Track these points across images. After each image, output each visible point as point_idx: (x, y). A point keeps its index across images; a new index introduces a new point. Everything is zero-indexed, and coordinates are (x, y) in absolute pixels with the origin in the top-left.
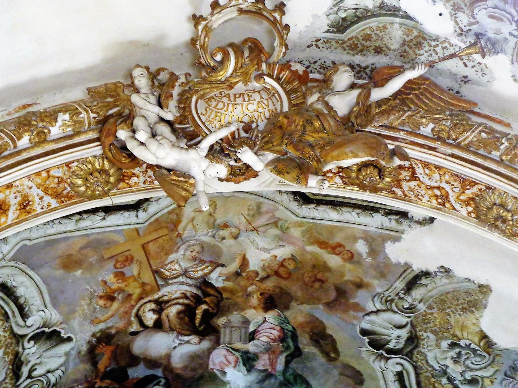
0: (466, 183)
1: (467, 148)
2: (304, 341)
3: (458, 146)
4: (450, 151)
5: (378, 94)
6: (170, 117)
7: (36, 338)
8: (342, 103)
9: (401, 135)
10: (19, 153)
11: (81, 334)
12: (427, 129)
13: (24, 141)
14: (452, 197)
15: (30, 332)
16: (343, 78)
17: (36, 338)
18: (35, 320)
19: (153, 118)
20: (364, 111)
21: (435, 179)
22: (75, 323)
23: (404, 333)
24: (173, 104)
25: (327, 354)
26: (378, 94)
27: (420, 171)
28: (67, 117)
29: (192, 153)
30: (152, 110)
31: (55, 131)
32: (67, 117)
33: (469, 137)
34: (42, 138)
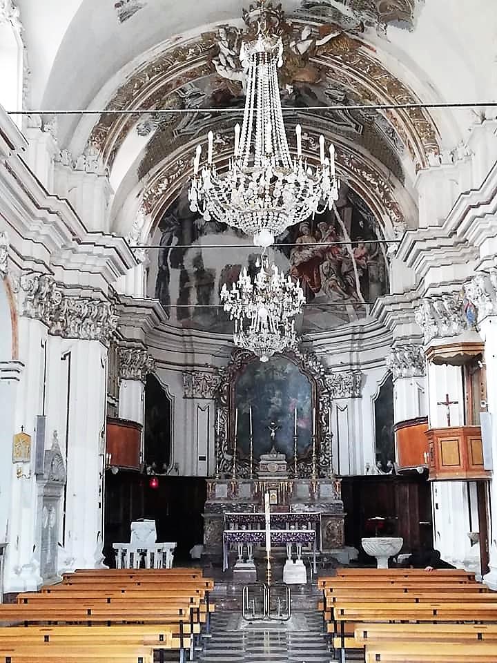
4: (347, 67)
5: (318, 43)
6: (233, 54)
8: (303, 48)
11: (208, 92)
15: (188, 96)
16: (305, 34)
17: (190, 97)
20: (313, 50)
22: (206, 90)
23: (343, 97)
25: (312, 97)
26: (318, 43)
27: (336, 71)
28: (193, 50)
30: (226, 51)
32: (193, 50)
33: (355, 62)
34: (184, 59)
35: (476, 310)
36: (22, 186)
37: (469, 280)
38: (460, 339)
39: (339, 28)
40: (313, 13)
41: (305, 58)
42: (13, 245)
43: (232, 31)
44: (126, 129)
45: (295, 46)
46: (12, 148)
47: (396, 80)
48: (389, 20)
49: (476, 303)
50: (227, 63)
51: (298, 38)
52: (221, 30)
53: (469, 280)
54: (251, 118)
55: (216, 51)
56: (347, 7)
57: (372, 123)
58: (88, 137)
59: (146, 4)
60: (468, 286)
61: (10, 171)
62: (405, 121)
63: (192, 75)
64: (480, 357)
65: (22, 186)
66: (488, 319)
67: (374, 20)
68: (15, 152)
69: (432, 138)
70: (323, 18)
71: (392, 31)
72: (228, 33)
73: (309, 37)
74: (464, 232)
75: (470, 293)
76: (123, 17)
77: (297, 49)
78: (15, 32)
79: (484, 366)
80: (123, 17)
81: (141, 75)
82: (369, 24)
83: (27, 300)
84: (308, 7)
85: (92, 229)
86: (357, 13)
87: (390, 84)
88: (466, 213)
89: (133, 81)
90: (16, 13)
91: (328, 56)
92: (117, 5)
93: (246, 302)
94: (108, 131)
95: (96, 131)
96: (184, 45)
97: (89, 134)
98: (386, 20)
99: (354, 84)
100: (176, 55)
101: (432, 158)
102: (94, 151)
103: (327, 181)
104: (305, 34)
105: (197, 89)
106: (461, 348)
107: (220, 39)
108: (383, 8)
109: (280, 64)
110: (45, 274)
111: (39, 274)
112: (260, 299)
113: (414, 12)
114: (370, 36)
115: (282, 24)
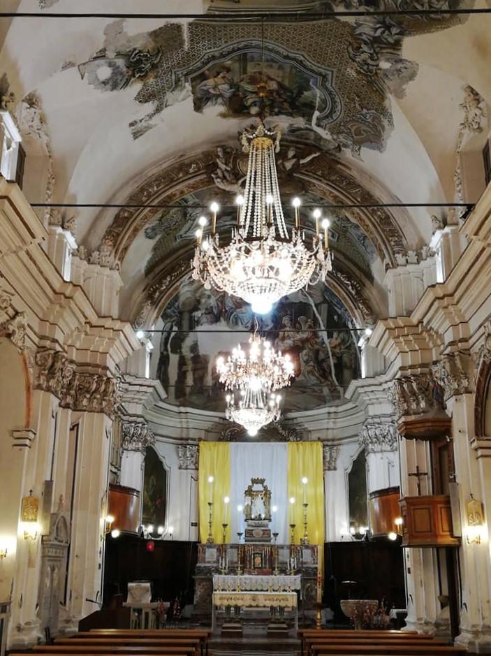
0: (331, 192)
1: (332, 182)
3: (329, 181)
4: (326, 182)
5: (302, 162)
6: (229, 169)
8: (289, 165)
9: (311, 174)
10: (178, 179)
12: (319, 173)
13: (181, 175)
14: (327, 194)
16: (291, 153)
18: (190, 203)
19: (223, 169)
20: (296, 168)
21: (321, 189)
24: (231, 165)
26: (302, 162)
29: (236, 186)
30: (223, 167)
31: (191, 171)
32: (195, 165)
33: (333, 178)
34: (187, 173)
35: (442, 390)
36: (41, 273)
37: (435, 363)
38: (430, 416)
39: (322, 150)
40: (297, 137)
42: (31, 324)
43: (229, 150)
44: (136, 230)
46: (34, 237)
47: (368, 193)
48: (363, 142)
49: (442, 384)
50: (224, 177)
52: (219, 149)
53: (435, 363)
54: (250, 208)
55: (216, 166)
56: (326, 132)
57: (346, 231)
58: (102, 236)
59: (156, 125)
60: (434, 369)
62: (376, 228)
63: (194, 187)
65: (41, 273)
66: (454, 398)
67: (349, 143)
69: (399, 243)
70: (309, 141)
71: (365, 151)
72: (225, 152)
73: (294, 157)
74: (429, 323)
75: (438, 375)
76: (136, 135)
77: (284, 167)
79: (451, 440)
80: (136, 135)
81: (150, 185)
82: (346, 146)
85: (74, 197)
86: (335, 137)
87: (363, 198)
88: (432, 304)
89: (142, 190)
91: (310, 172)
92: (131, 125)
93: (239, 375)
94: (119, 231)
95: (109, 232)
96: (186, 162)
97: (104, 233)
98: (359, 143)
99: (332, 197)
101: (400, 259)
102: (107, 249)
104: (291, 153)
105: (197, 200)
106: (430, 424)
107: (218, 157)
108: (358, 133)
109: (278, 150)
110: (57, 341)
111: (52, 352)
112: (253, 371)
113: (385, 135)
114: (347, 153)
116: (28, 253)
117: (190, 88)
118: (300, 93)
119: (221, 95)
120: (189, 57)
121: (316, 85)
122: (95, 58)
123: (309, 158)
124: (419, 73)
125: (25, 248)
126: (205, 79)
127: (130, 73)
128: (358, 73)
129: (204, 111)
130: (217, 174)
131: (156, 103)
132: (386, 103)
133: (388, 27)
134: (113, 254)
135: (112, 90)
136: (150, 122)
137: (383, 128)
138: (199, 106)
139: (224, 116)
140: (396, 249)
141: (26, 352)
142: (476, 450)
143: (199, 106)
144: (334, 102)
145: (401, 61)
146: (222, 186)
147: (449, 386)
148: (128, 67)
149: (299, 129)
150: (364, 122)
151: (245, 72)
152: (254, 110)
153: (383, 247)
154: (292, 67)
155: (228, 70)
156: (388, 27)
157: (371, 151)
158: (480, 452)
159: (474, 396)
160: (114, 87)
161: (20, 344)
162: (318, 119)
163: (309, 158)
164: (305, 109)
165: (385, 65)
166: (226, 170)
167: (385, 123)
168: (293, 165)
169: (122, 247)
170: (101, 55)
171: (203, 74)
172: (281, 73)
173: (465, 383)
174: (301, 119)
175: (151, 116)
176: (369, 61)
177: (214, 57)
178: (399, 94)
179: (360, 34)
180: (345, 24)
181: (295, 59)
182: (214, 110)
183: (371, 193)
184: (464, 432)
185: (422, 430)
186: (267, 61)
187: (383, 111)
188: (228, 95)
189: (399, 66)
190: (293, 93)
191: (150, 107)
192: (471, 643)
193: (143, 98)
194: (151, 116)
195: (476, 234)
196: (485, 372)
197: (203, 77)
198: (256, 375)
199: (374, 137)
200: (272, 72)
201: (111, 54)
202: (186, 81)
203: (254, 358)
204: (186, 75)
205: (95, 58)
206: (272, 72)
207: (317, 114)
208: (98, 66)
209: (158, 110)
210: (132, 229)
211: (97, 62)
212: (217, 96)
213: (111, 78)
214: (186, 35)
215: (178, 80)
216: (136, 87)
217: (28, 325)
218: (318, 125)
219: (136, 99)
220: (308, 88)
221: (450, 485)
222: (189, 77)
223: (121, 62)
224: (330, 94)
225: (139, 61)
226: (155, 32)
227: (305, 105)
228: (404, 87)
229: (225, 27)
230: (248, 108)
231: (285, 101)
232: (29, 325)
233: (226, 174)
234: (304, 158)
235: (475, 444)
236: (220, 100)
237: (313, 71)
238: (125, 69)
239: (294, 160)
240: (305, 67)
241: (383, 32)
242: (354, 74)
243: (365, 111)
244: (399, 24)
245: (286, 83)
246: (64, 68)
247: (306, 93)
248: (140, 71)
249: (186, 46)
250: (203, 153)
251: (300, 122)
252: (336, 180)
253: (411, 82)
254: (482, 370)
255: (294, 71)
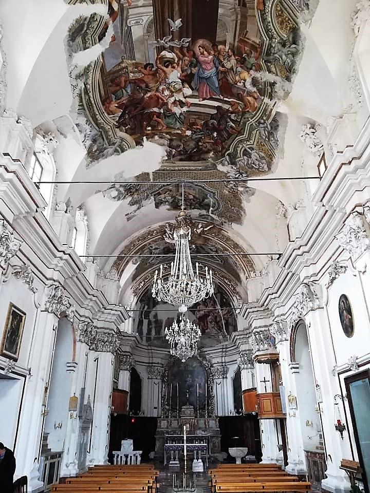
2: (199, 248)
7: (154, 249)
8: (199, 231)
11: (162, 247)
16: (200, 226)
17: (154, 249)
18: (154, 248)
20: (203, 232)
26: (205, 229)
30: (169, 232)
33: (219, 237)
34: (152, 235)
35: (275, 339)
37: (271, 325)
38: (269, 352)
39: (213, 224)
40: (203, 218)
41: (200, 235)
42: (78, 311)
45: (196, 230)
46: (80, 270)
47: (236, 244)
49: (274, 335)
50: (169, 237)
51: (197, 228)
53: (271, 325)
55: (165, 232)
61: (78, 279)
63: (155, 241)
64: (278, 360)
66: (280, 342)
68: (81, 272)
69: (252, 266)
70: (208, 220)
72: (169, 226)
73: (201, 227)
74: (267, 305)
75: (272, 331)
76: (128, 219)
78: (85, 225)
80: (128, 219)
81: (134, 241)
82: (225, 222)
83: (81, 334)
84: (201, 216)
89: (131, 243)
90: (86, 218)
92: (126, 215)
93: (176, 336)
95: (115, 263)
96: (152, 230)
97: (112, 264)
98: (232, 221)
100: (149, 234)
102: (114, 271)
103: (209, 285)
104: (200, 226)
105: (157, 246)
106: (269, 356)
107: (167, 228)
108: (230, 217)
109: (190, 239)
111: (87, 323)
113: (242, 218)
115: (191, 222)
116: (77, 277)
117: (153, 199)
118: (203, 200)
119: (166, 202)
120: (152, 186)
121: (210, 196)
122: (111, 188)
123: (209, 228)
124: (256, 192)
125: (76, 275)
126: (160, 195)
127: (126, 193)
128: (229, 192)
129: (160, 208)
130: (166, 236)
131: (138, 205)
132: (242, 205)
133: (241, 174)
134: (117, 274)
135: (118, 201)
136: (135, 214)
137: (242, 215)
138: (157, 206)
139: (169, 210)
140: (250, 269)
141: (74, 324)
142: (291, 369)
143: (157, 206)
144: (219, 204)
145: (248, 187)
146: (168, 241)
147: (278, 337)
148: (125, 191)
149: (204, 215)
150: (233, 213)
151: (178, 191)
152: (183, 207)
153: (244, 269)
154: (200, 189)
155: (171, 191)
156: (241, 174)
157: (236, 225)
158: (294, 370)
159: (289, 341)
160: (119, 200)
161: (72, 320)
162: (212, 211)
163: (209, 228)
164: (206, 207)
165: (240, 189)
166: (170, 233)
167: (242, 213)
168: (201, 231)
169: (121, 270)
170: (113, 187)
171: (159, 192)
172: (194, 192)
173: (285, 336)
174: (204, 211)
175: (135, 211)
176: (234, 187)
177: (164, 186)
178: (249, 201)
179: (229, 176)
180: (222, 172)
181: (200, 186)
182: (164, 208)
183: (238, 243)
184: (286, 361)
185: (266, 359)
186: (188, 187)
187: (242, 208)
188: (171, 201)
189: (247, 189)
190: (200, 200)
191: (135, 207)
192: (293, 470)
193: (132, 204)
194: (135, 211)
195: (284, 267)
196: (293, 330)
197: (159, 194)
198: (183, 336)
199: (236, 218)
200: (191, 192)
201: (117, 186)
202: (151, 196)
203: (182, 328)
204: (152, 193)
205: (111, 188)
206: (191, 192)
207: (211, 209)
208: (112, 191)
209: (138, 208)
210: (126, 261)
211: (112, 189)
212: (166, 202)
213: (118, 196)
214: (151, 177)
215: (148, 195)
216: (130, 199)
217: (76, 311)
218: (212, 213)
219: (128, 204)
220: (207, 198)
221: (280, 386)
222: (153, 194)
223: (122, 189)
224: (217, 200)
225: (130, 188)
226: (138, 176)
227: (206, 205)
228: (250, 198)
229: (169, 173)
230: (180, 206)
231: (197, 203)
232: (76, 311)
233: (170, 235)
234: (206, 228)
235: (291, 366)
236: (167, 203)
237: (209, 191)
238: (124, 192)
239: (202, 229)
240: (205, 189)
241: (239, 176)
242: (227, 192)
243: (233, 208)
244: (246, 172)
245: (197, 196)
246: (96, 193)
247: (206, 200)
248: (131, 192)
249: (152, 181)
250: (159, 226)
251: (204, 212)
252: (221, 237)
253: (253, 196)
254: (292, 329)
255: (200, 191)
